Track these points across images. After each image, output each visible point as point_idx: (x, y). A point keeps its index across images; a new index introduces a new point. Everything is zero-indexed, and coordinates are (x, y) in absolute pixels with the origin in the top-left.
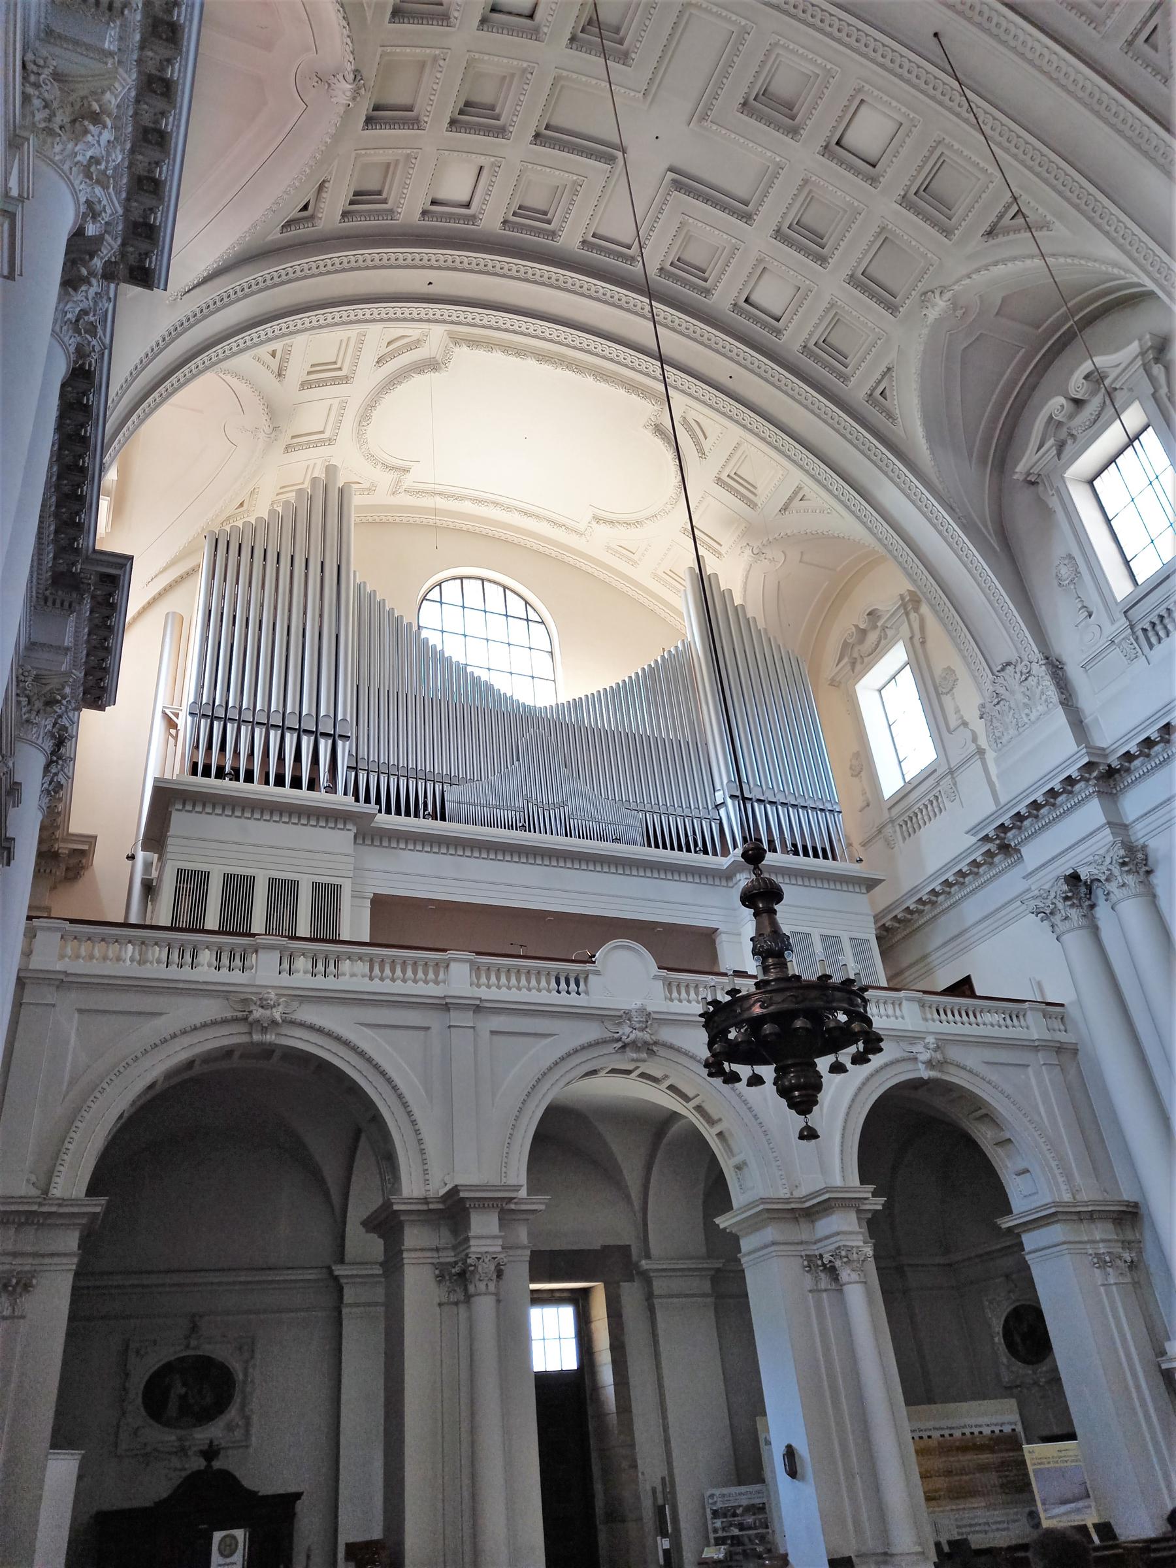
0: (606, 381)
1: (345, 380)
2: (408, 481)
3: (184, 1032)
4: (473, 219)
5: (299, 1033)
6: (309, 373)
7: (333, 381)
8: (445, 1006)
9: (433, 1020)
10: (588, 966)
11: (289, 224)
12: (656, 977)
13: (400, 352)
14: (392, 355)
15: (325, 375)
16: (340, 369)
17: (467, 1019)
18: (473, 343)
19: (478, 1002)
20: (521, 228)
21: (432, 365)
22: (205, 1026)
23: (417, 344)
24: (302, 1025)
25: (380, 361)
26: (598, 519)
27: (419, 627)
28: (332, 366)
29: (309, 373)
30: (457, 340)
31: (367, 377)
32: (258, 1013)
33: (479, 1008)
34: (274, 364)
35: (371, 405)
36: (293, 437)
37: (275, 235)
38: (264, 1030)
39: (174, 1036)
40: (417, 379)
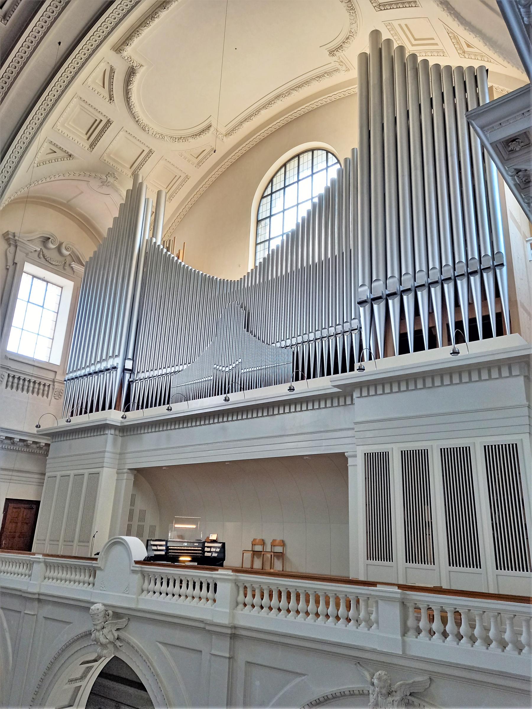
6: (88, 139)
7: (103, 131)
12: (134, 572)
13: (111, 84)
14: (111, 90)
15: (97, 130)
16: (101, 120)
18: (127, 40)
21: (131, 72)
23: (112, 71)
25: (111, 98)
28: (96, 123)
29: (88, 139)
30: (118, 48)
31: (116, 111)
34: (60, 154)
36: (131, 168)
40: (134, 87)
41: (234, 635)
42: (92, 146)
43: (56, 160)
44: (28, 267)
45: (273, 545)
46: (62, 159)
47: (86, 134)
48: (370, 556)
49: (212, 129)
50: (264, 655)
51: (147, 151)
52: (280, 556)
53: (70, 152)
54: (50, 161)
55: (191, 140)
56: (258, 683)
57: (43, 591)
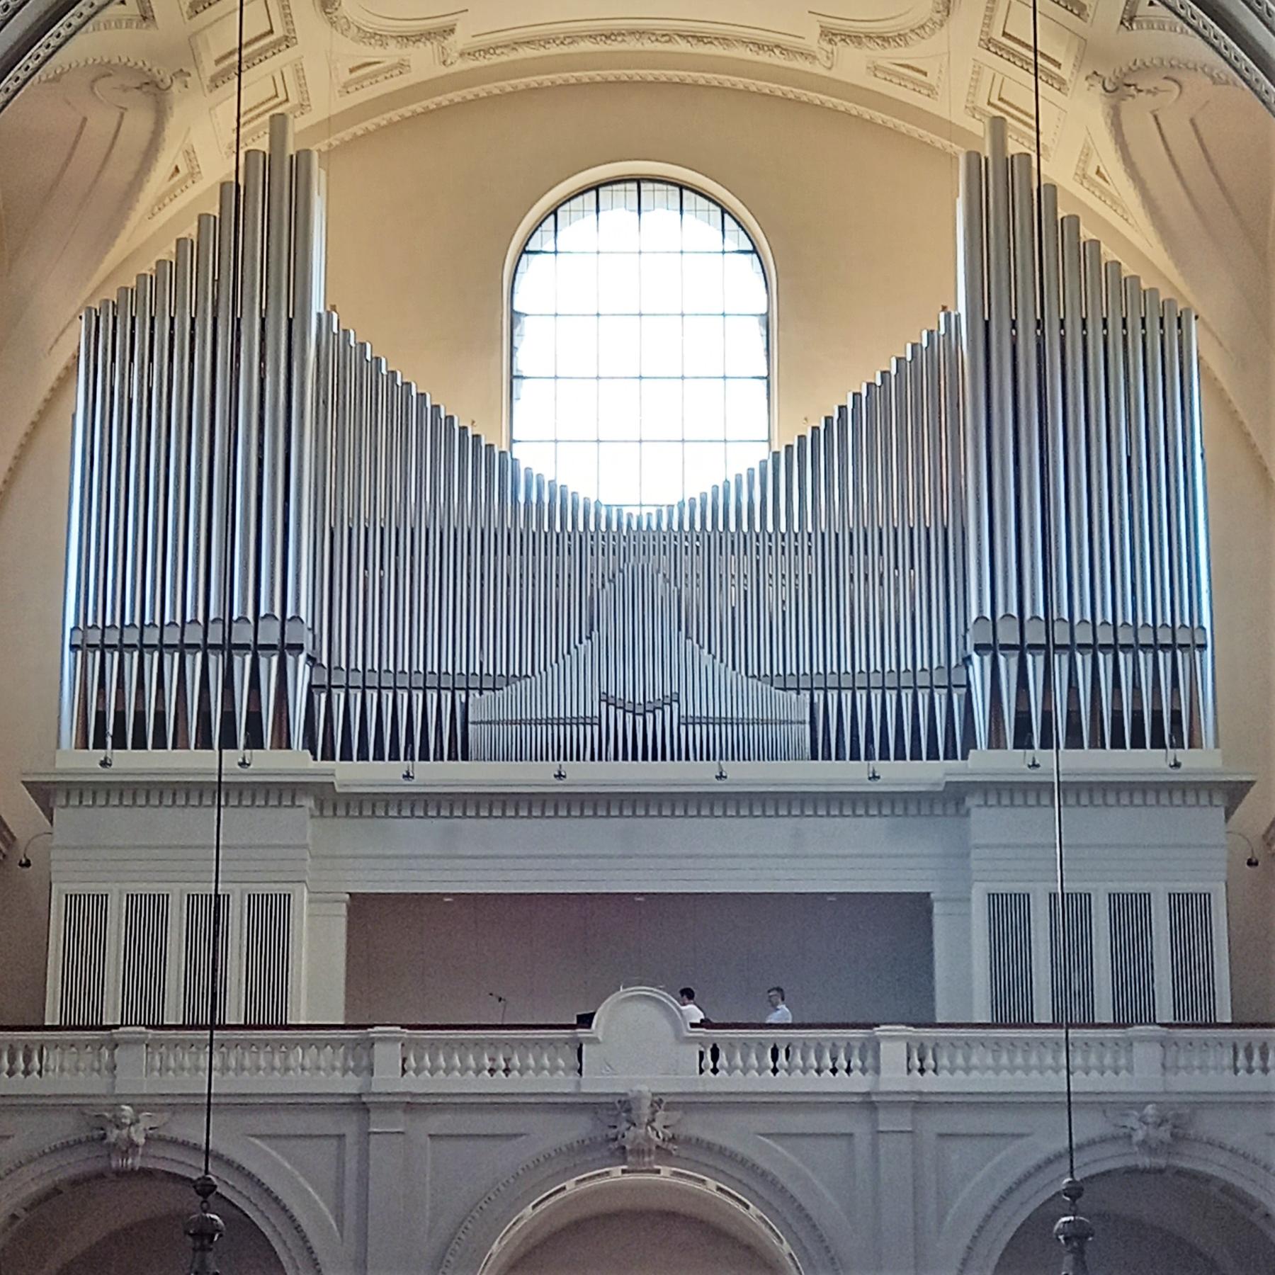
2: (460, 40)
3: (31, 1160)
5: (171, 1153)
8: (360, 1105)
9: (349, 1126)
10: (582, 1033)
19: (408, 1099)
24: (173, 1142)
26: (828, 34)
32: (113, 1135)
33: (413, 1105)
38: (125, 1154)
41: (920, 1104)
49: (451, 38)
55: (392, 43)
56: (955, 1157)
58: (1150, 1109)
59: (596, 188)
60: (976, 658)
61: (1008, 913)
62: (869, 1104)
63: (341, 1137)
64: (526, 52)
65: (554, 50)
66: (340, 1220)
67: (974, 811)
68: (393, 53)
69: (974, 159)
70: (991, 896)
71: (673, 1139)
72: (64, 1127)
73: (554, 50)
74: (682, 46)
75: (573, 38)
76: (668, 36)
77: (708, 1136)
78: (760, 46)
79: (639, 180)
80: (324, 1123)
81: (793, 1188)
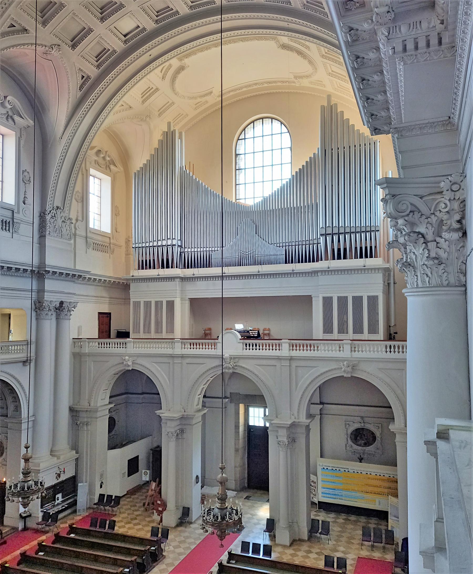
0: (248, 40)
1: (157, 89)
4: (144, 29)
6: (142, 97)
8: (172, 356)
9: (170, 361)
11: (81, 88)
17: (179, 361)
18: (187, 56)
20: (164, 19)
21: (182, 68)
22: (116, 365)
23: (170, 66)
24: (137, 364)
27: (237, 155)
29: (142, 97)
33: (183, 357)
35: (173, 89)
37: (79, 94)
39: (110, 368)
42: (143, 102)
43: (123, 110)
44: (92, 171)
45: (264, 330)
46: (126, 110)
47: (142, 94)
48: (324, 333)
49: (212, 94)
50: (302, 363)
51: (170, 102)
52: (269, 334)
53: (131, 106)
54: (120, 112)
56: (300, 371)
57: (183, 353)
58: (345, 363)
59: (253, 122)
60: (321, 238)
61: (327, 301)
62: (279, 358)
63: (169, 363)
64: (232, 93)
65: (238, 91)
66: (169, 381)
67: (320, 276)
68: (203, 99)
69: (323, 107)
70: (324, 298)
71: (236, 366)
72: (118, 360)
73: (238, 91)
74: (266, 85)
75: (242, 88)
76: (262, 83)
77: (243, 366)
78: (283, 82)
79: (262, 118)
80: (166, 360)
81: (263, 378)
